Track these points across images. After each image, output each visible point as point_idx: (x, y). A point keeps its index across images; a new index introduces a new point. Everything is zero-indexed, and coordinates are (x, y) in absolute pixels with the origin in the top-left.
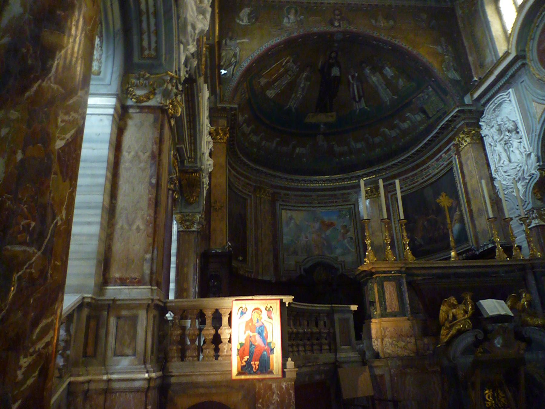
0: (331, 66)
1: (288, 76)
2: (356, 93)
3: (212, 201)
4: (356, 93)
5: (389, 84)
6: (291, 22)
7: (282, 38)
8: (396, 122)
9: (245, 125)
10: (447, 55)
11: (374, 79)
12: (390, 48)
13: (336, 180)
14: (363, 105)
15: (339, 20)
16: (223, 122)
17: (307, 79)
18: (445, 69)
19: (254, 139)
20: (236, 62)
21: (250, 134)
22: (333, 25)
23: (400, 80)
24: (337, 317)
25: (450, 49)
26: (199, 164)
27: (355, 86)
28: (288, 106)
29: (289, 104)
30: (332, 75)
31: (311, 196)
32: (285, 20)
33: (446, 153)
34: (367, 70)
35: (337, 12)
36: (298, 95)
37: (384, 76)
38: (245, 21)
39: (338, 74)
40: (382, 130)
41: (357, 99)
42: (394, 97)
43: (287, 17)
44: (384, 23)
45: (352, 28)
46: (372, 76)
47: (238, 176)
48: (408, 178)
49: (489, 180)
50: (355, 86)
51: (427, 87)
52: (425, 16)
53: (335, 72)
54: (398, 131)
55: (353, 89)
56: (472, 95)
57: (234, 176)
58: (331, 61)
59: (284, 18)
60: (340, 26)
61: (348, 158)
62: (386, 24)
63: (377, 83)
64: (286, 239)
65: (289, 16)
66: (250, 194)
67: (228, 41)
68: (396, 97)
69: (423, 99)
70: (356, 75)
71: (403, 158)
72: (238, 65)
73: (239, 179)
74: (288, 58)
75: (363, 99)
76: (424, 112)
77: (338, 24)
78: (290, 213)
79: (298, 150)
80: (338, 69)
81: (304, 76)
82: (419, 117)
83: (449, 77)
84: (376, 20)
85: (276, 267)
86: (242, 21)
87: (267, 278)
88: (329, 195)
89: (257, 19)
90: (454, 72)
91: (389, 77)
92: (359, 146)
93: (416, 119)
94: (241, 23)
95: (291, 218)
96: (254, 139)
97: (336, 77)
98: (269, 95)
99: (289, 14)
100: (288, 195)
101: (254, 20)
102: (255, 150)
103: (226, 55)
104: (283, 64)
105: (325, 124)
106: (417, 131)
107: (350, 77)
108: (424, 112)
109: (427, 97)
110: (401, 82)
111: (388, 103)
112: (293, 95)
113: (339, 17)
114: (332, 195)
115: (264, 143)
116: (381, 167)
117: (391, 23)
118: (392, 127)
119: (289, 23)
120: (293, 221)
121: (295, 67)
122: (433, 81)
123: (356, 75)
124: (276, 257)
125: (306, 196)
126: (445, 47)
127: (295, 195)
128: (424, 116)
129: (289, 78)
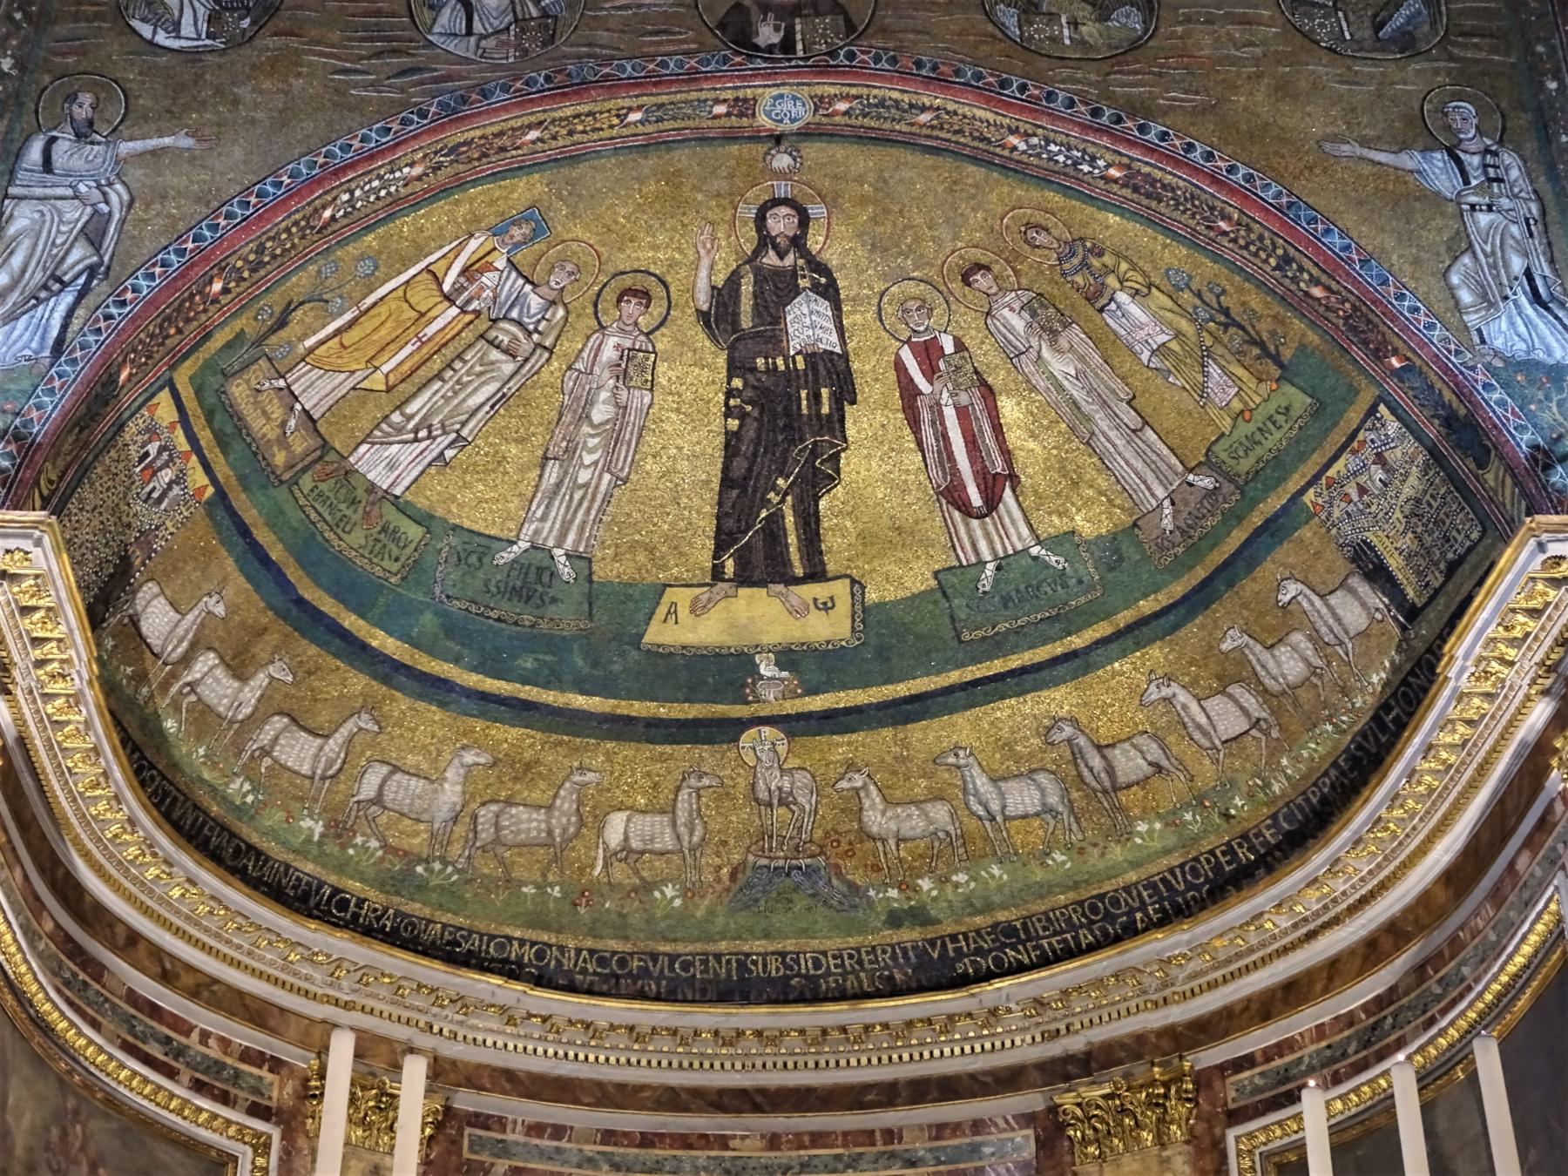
1: (495, 355)
6: (478, 27)
7: (405, 122)
9: (206, 662)
12: (1114, 172)
14: (1019, 536)
20: (92, 271)
21: (256, 720)
23: (1214, 370)
25: (1512, 166)
27: (950, 413)
28: (524, 545)
29: (529, 529)
30: (794, 345)
31: (723, 1142)
32: (449, 17)
33: (1530, 843)
34: (1006, 312)
36: (584, 476)
37: (1108, 344)
38: (187, 29)
39: (831, 341)
41: (976, 500)
42: (1191, 477)
44: (1074, 24)
46: (1046, 353)
50: (950, 413)
51: (1373, 410)
54: (1250, 702)
58: (771, 259)
61: (961, 878)
62: (1089, 30)
63: (1078, 395)
67: (61, 149)
68: (1206, 482)
69: (1362, 490)
72: (100, 287)
74: (473, 244)
75: (1008, 493)
77: (776, 39)
80: (824, 306)
81: (609, 353)
83: (1499, 343)
86: (175, 29)
88: (848, 1137)
90: (1529, 310)
91: (1145, 356)
93: (1338, 620)
94: (161, 38)
97: (812, 358)
98: (379, 476)
100: (559, 1132)
101: (246, 23)
102: (314, 827)
104: (446, 287)
105: (787, 657)
106: (1359, 703)
107: (907, 356)
109: (1379, 474)
111: (1168, 523)
114: (868, 1136)
119: (470, 31)
121: (535, 302)
122: (1395, 373)
125: (684, 1141)
126: (1476, 160)
127: (609, 1136)
128: (1377, 600)
129: (509, 368)
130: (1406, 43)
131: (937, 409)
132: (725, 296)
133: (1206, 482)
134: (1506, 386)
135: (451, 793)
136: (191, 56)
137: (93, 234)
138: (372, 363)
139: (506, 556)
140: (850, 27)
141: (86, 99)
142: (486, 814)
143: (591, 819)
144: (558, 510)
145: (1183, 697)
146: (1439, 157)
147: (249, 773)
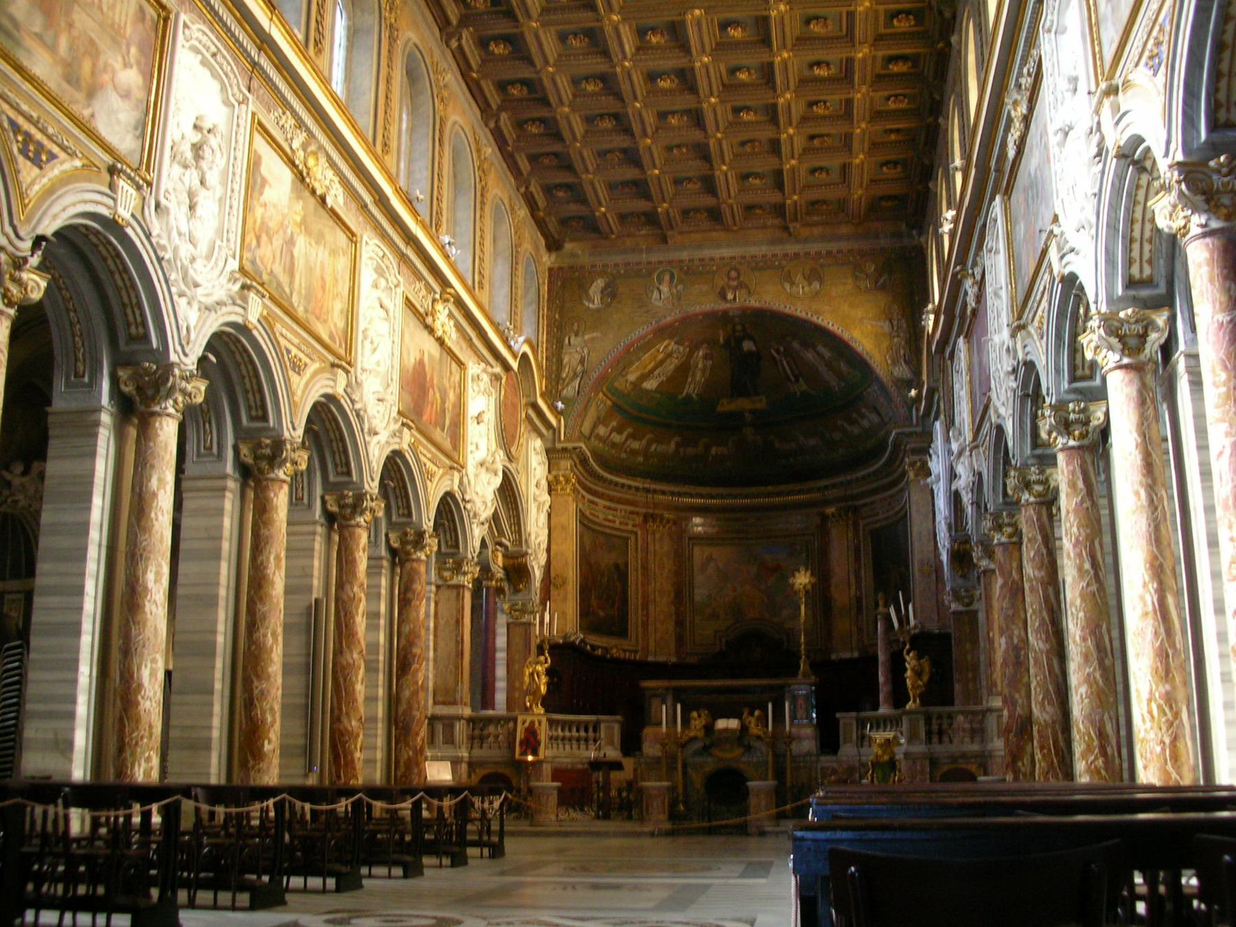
0: (739, 341)
2: (789, 372)
3: (553, 575)
4: (789, 372)
5: (829, 365)
8: (854, 415)
10: (898, 336)
11: (809, 356)
13: (789, 493)
14: (804, 387)
15: (735, 289)
16: (566, 464)
17: (706, 357)
18: (889, 362)
19: (636, 445)
22: (723, 296)
24: (603, 726)
26: (524, 548)
32: (656, 293)
35: (733, 274)
39: (754, 348)
40: (839, 422)
41: (792, 378)
43: (658, 289)
44: (803, 288)
45: (754, 303)
47: (612, 505)
48: (885, 499)
49: (932, 537)
52: (871, 268)
53: (748, 345)
55: (782, 365)
56: (918, 410)
57: (605, 507)
59: (653, 292)
60: (735, 298)
62: (807, 289)
64: (700, 594)
65: (661, 288)
66: (635, 529)
70: (782, 349)
71: (876, 467)
72: (585, 377)
73: (615, 510)
76: (879, 414)
78: (708, 551)
79: (714, 450)
81: (701, 353)
82: (875, 419)
83: (895, 374)
84: (792, 283)
85: (680, 640)
86: (593, 303)
87: (661, 659)
89: (613, 296)
92: (812, 442)
95: (710, 559)
96: (636, 445)
97: (750, 353)
99: (660, 283)
102: (641, 459)
103: (569, 362)
105: (751, 411)
108: (879, 414)
110: (843, 367)
112: (690, 379)
113: (735, 283)
115: (653, 448)
116: (849, 478)
117: (816, 285)
118: (853, 422)
120: (712, 564)
123: (782, 349)
124: (679, 623)
130: (883, 288)
131: (781, 361)
132: (727, 341)
133: (843, 384)
134: (896, 386)
135: (673, 446)
136: (598, 310)
137: (582, 361)
138: (645, 368)
139: (680, 397)
140: (749, 292)
141: (576, 325)
142: (681, 450)
143: (707, 447)
144: (692, 386)
145: (846, 425)
146: (887, 322)
147: (625, 451)
